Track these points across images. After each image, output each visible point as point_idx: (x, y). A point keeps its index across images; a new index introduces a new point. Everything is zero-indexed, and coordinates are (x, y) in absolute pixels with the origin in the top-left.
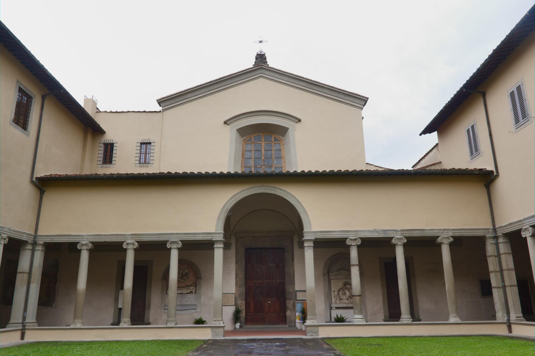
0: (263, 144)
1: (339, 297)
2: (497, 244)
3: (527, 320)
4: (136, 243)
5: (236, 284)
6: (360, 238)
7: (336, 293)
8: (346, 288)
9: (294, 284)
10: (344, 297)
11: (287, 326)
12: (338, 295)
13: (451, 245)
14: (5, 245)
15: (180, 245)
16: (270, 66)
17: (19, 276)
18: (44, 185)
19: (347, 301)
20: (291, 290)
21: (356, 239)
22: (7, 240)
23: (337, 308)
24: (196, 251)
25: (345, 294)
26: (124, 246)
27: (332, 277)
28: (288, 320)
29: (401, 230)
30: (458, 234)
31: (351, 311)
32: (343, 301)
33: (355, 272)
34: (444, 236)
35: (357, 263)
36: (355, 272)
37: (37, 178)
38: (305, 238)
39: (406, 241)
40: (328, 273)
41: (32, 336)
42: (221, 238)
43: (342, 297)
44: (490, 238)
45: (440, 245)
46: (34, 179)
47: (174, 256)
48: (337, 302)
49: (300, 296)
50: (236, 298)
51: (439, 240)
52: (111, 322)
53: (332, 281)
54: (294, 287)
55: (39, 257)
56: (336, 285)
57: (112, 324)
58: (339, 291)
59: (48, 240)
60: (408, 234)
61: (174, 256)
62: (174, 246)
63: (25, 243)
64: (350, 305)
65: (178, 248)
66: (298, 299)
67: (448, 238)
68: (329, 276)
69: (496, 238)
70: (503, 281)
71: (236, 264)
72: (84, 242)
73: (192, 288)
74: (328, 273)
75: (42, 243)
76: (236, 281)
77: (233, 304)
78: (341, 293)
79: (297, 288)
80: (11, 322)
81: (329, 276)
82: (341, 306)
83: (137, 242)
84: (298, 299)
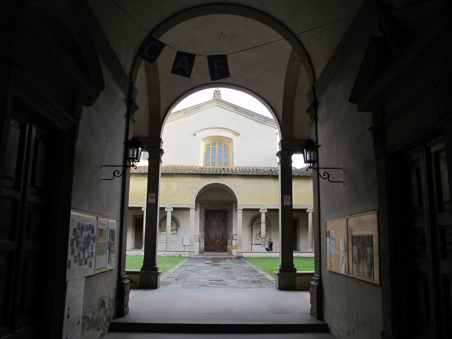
0: (217, 148)
7: (255, 236)
10: (260, 239)
11: (227, 253)
16: (223, 99)
20: (230, 234)
27: (253, 228)
28: (228, 250)
31: (260, 246)
33: (263, 226)
35: (264, 221)
36: (263, 226)
40: (252, 225)
42: (194, 207)
49: (235, 237)
50: (199, 238)
51: (307, 211)
53: (254, 230)
54: (232, 233)
56: (255, 232)
58: (257, 235)
62: (169, 210)
68: (252, 227)
73: (175, 232)
74: (252, 225)
78: (258, 236)
81: (252, 227)
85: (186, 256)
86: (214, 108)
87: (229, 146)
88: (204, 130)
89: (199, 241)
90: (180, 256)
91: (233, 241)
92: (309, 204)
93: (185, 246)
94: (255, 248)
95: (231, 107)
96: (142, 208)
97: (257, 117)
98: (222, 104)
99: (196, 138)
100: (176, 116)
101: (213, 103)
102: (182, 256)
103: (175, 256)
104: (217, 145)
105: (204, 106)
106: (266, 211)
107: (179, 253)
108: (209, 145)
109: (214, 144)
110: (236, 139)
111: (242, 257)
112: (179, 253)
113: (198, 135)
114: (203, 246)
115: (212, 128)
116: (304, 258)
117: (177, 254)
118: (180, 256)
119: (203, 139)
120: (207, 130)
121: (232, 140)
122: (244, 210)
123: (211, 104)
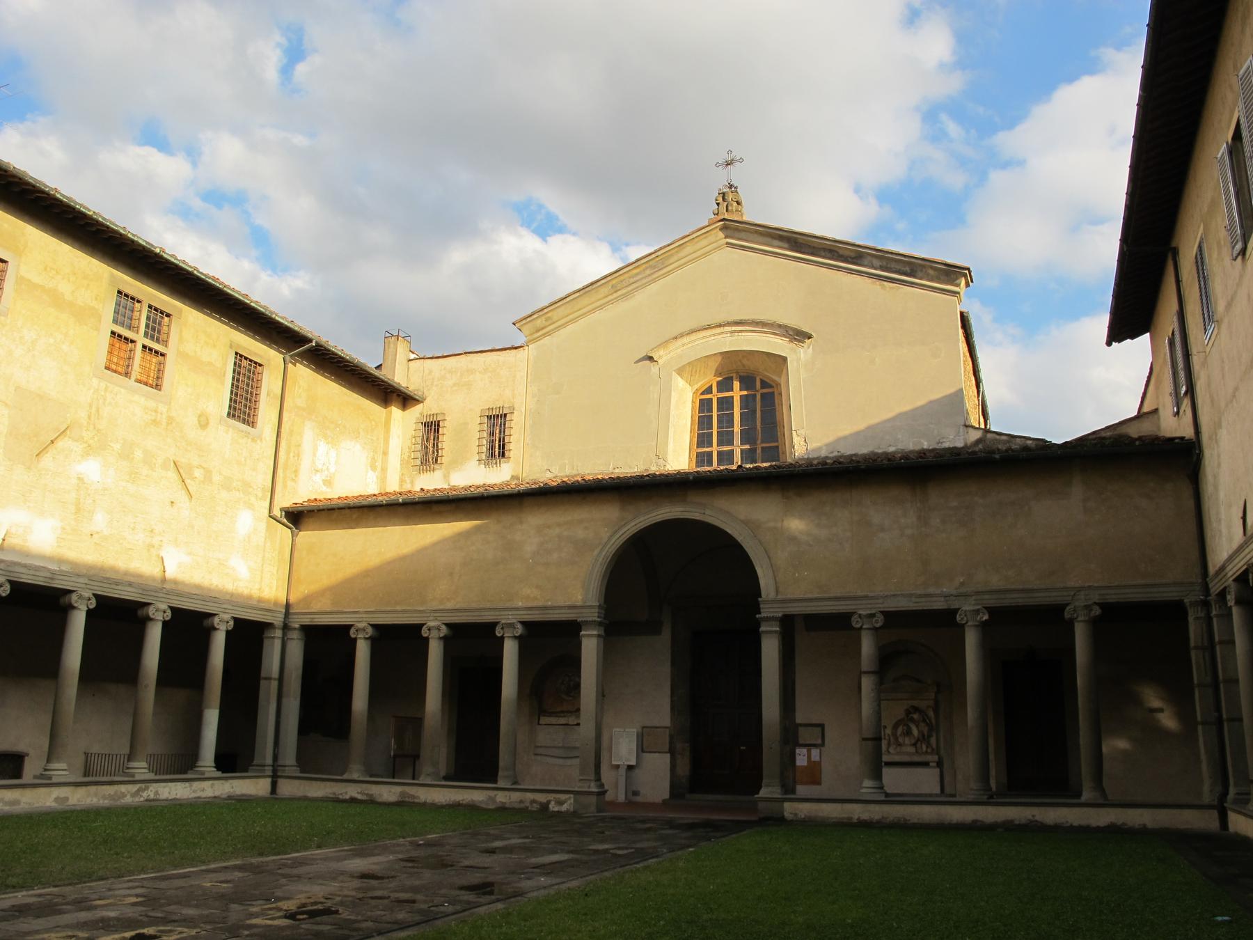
1: (896, 739)
2: (1209, 619)
3: (302, 772)
4: (444, 627)
5: (672, 709)
6: (885, 613)
7: (888, 731)
8: (912, 720)
9: (794, 710)
10: (907, 741)
12: (894, 734)
13: (1096, 625)
14: (228, 632)
15: (519, 630)
17: (263, 683)
18: (296, 517)
19: (912, 750)
21: (872, 616)
22: (232, 623)
23: (889, 764)
24: (550, 641)
25: (908, 733)
26: (425, 633)
29: (978, 593)
30: (1113, 597)
32: (905, 749)
34: (1077, 604)
37: (281, 510)
38: (763, 615)
39: (986, 617)
41: (288, 788)
42: (593, 615)
43: (901, 740)
44: (1193, 604)
45: (1071, 623)
46: (277, 513)
47: (510, 651)
48: (891, 750)
50: (671, 737)
52: (443, 773)
55: (296, 650)
57: (446, 778)
58: (895, 727)
59: (306, 621)
60: (992, 601)
61: (510, 651)
63: (269, 626)
64: (916, 759)
65: (515, 637)
66: (801, 742)
67: (1088, 608)
69: (1206, 604)
70: (1218, 709)
71: (673, 664)
72: (361, 625)
75: (297, 626)
76: (672, 701)
77: (667, 748)
79: (798, 721)
80: (255, 762)
82: (897, 759)
83: (447, 625)
84: (801, 742)
85: (564, 808)
86: (716, 256)
87: (778, 385)
88: (682, 335)
89: (672, 751)
90: (544, 807)
91: (798, 751)
92: (1071, 584)
93: (618, 767)
94: (894, 779)
95: (776, 242)
96: (420, 626)
97: (876, 262)
98: (743, 235)
99: (654, 369)
100: (585, 301)
101: (711, 238)
102: (553, 807)
103: (525, 810)
104: (736, 385)
105: (682, 254)
106: (879, 621)
107: (542, 798)
108: (709, 390)
109: (725, 385)
110: (798, 358)
111: (780, 820)
112: (542, 798)
113: (662, 356)
114: (684, 769)
115: (710, 327)
116: (1056, 829)
117: (533, 801)
118: (544, 807)
119: (680, 372)
120: (694, 337)
121: (785, 359)
122: (788, 624)
123: (704, 242)
